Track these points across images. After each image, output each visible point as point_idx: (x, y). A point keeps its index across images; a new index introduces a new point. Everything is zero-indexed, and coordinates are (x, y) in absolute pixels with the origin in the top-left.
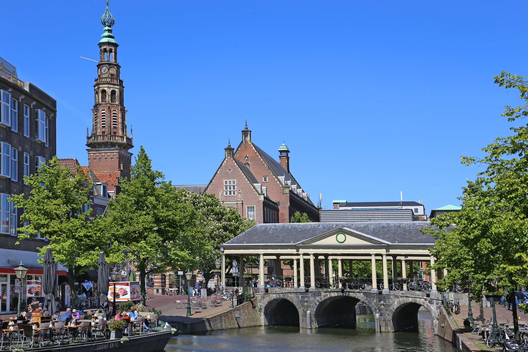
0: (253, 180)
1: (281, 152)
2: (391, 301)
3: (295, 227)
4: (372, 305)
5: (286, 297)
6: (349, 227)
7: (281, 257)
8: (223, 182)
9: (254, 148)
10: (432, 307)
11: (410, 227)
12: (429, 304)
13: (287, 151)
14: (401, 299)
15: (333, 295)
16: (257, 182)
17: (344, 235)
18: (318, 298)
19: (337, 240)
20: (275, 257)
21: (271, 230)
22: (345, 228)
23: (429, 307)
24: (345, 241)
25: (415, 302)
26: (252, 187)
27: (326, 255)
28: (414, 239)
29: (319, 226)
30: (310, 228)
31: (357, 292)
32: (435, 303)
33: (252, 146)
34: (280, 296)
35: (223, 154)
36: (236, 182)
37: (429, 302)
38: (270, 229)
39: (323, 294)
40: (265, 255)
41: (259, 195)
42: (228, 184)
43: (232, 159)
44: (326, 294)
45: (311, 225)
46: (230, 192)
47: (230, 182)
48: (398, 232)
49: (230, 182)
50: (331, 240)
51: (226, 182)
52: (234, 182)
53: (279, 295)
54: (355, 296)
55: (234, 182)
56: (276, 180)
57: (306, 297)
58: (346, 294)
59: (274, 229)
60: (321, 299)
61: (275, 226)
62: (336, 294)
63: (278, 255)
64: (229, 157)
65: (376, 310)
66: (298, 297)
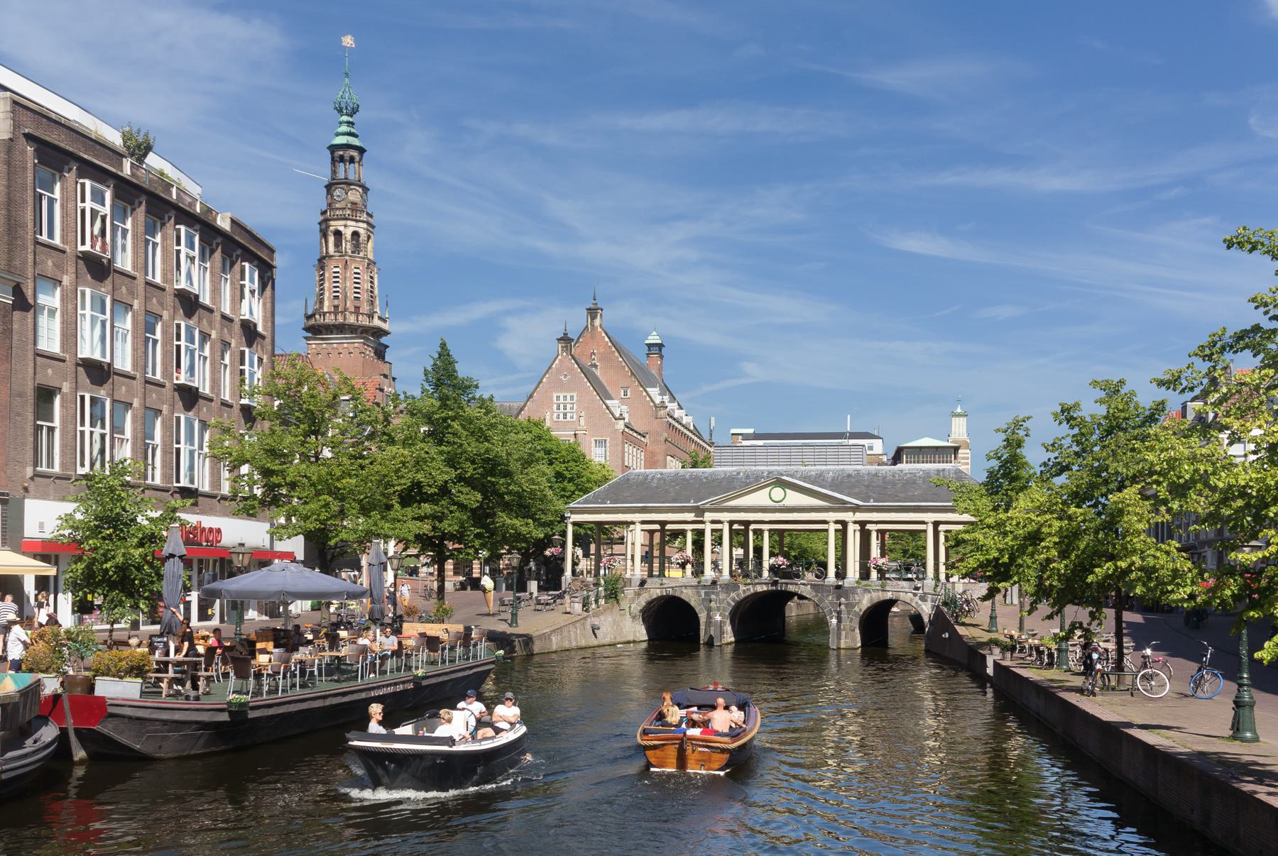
0: (604, 394)
1: (650, 346)
2: (857, 598)
3: (697, 476)
4: (825, 605)
5: (677, 594)
6: (792, 476)
7: (669, 527)
8: (552, 397)
9: (607, 339)
10: (924, 607)
11: (894, 476)
12: (920, 602)
13: (660, 346)
14: (874, 595)
15: (759, 589)
16: (611, 398)
18: (733, 595)
19: (771, 498)
20: (657, 527)
21: (655, 481)
22: (784, 478)
23: (920, 606)
24: (783, 499)
26: (604, 407)
27: (747, 523)
28: (901, 495)
29: (739, 473)
30: (724, 478)
31: (801, 584)
32: (929, 600)
33: (604, 334)
36: (575, 398)
38: (652, 479)
39: (742, 588)
40: (643, 522)
41: (616, 419)
42: (562, 399)
44: (748, 587)
45: (725, 472)
46: (565, 415)
47: (565, 397)
48: (874, 484)
49: (565, 397)
50: (760, 498)
51: (558, 397)
52: (572, 397)
55: (572, 397)
56: (644, 394)
57: (713, 593)
58: (781, 587)
59: (659, 479)
60: (738, 595)
61: (661, 474)
62: (765, 588)
63: (663, 523)
64: (565, 354)
65: (831, 613)
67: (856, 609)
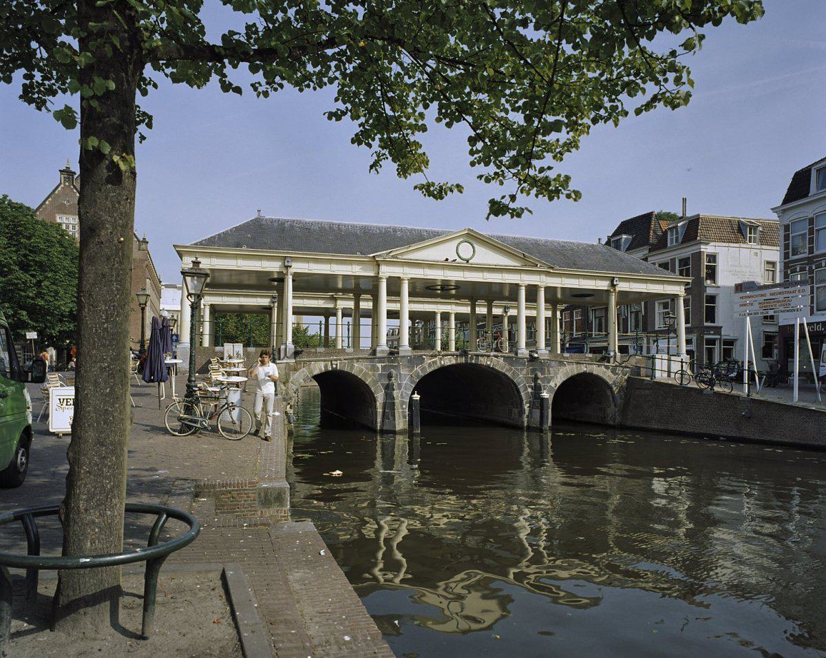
14: (568, 367)
17: (473, 247)
18: (417, 369)
25: (591, 372)
34: (334, 366)
35: (57, 178)
37: (612, 372)
39: (428, 361)
43: (72, 187)
53: (332, 364)
54: (489, 363)
58: (472, 358)
64: (67, 184)
66: (374, 368)
67: (552, 384)
